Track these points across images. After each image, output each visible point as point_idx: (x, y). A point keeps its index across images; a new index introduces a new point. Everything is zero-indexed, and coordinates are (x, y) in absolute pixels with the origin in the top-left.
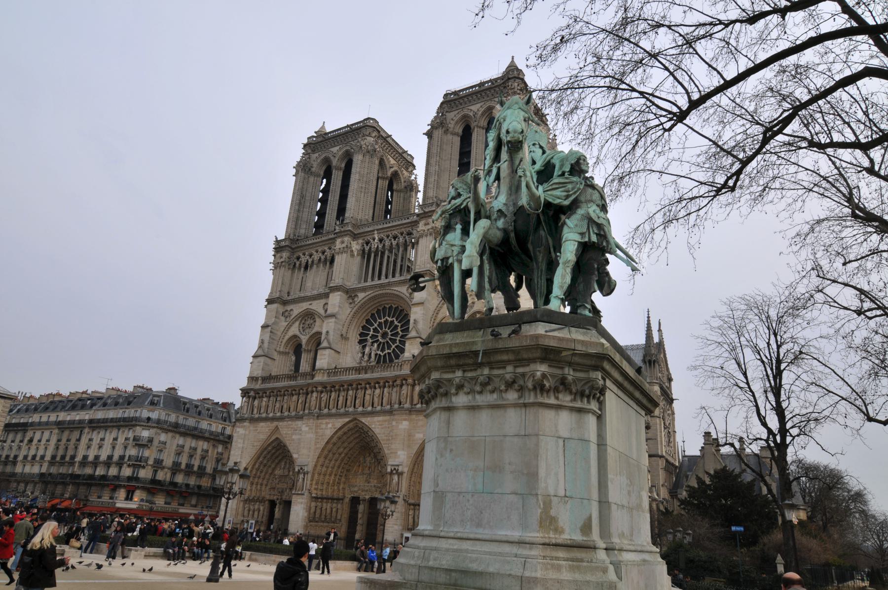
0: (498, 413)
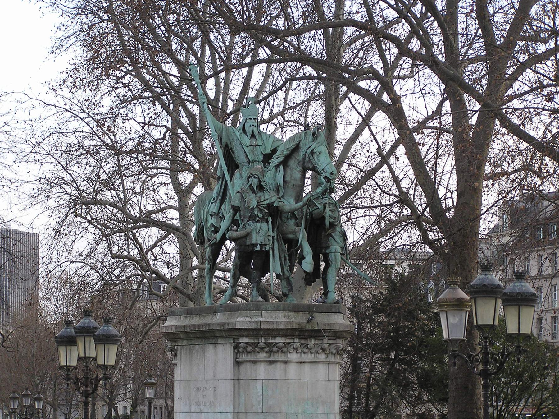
0: (314, 366)
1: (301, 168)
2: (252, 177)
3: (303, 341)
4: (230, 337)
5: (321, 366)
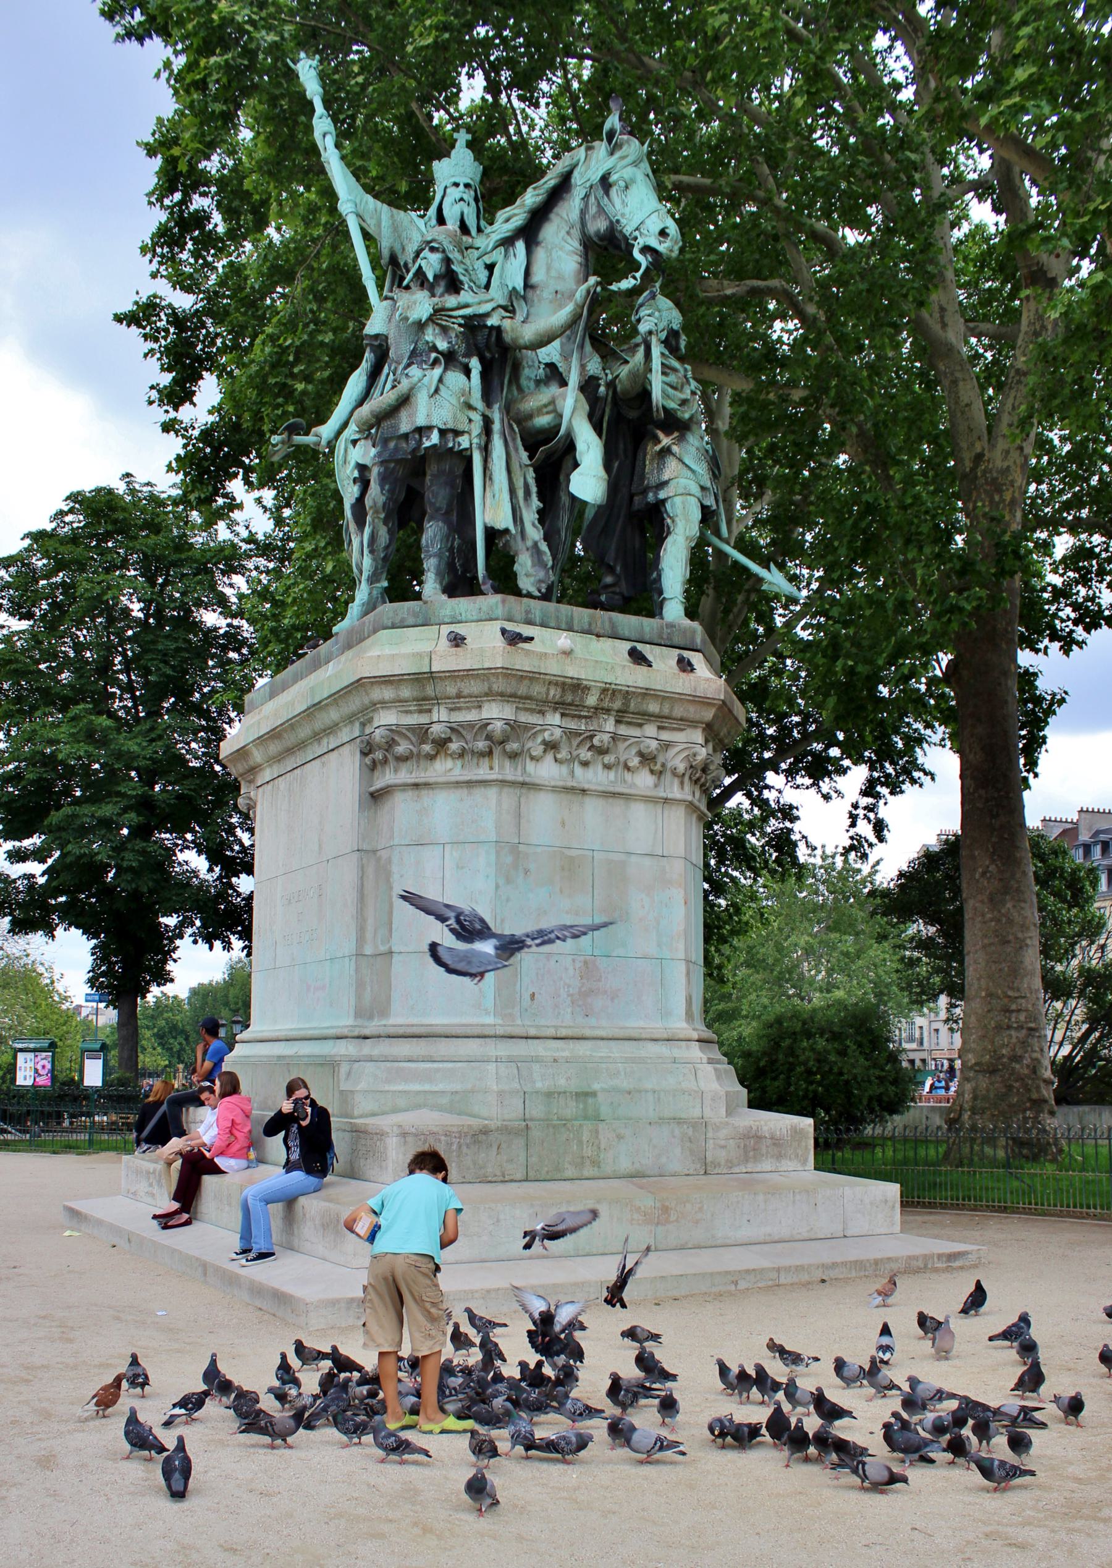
0: (618, 806)
3: (572, 725)
5: (639, 812)
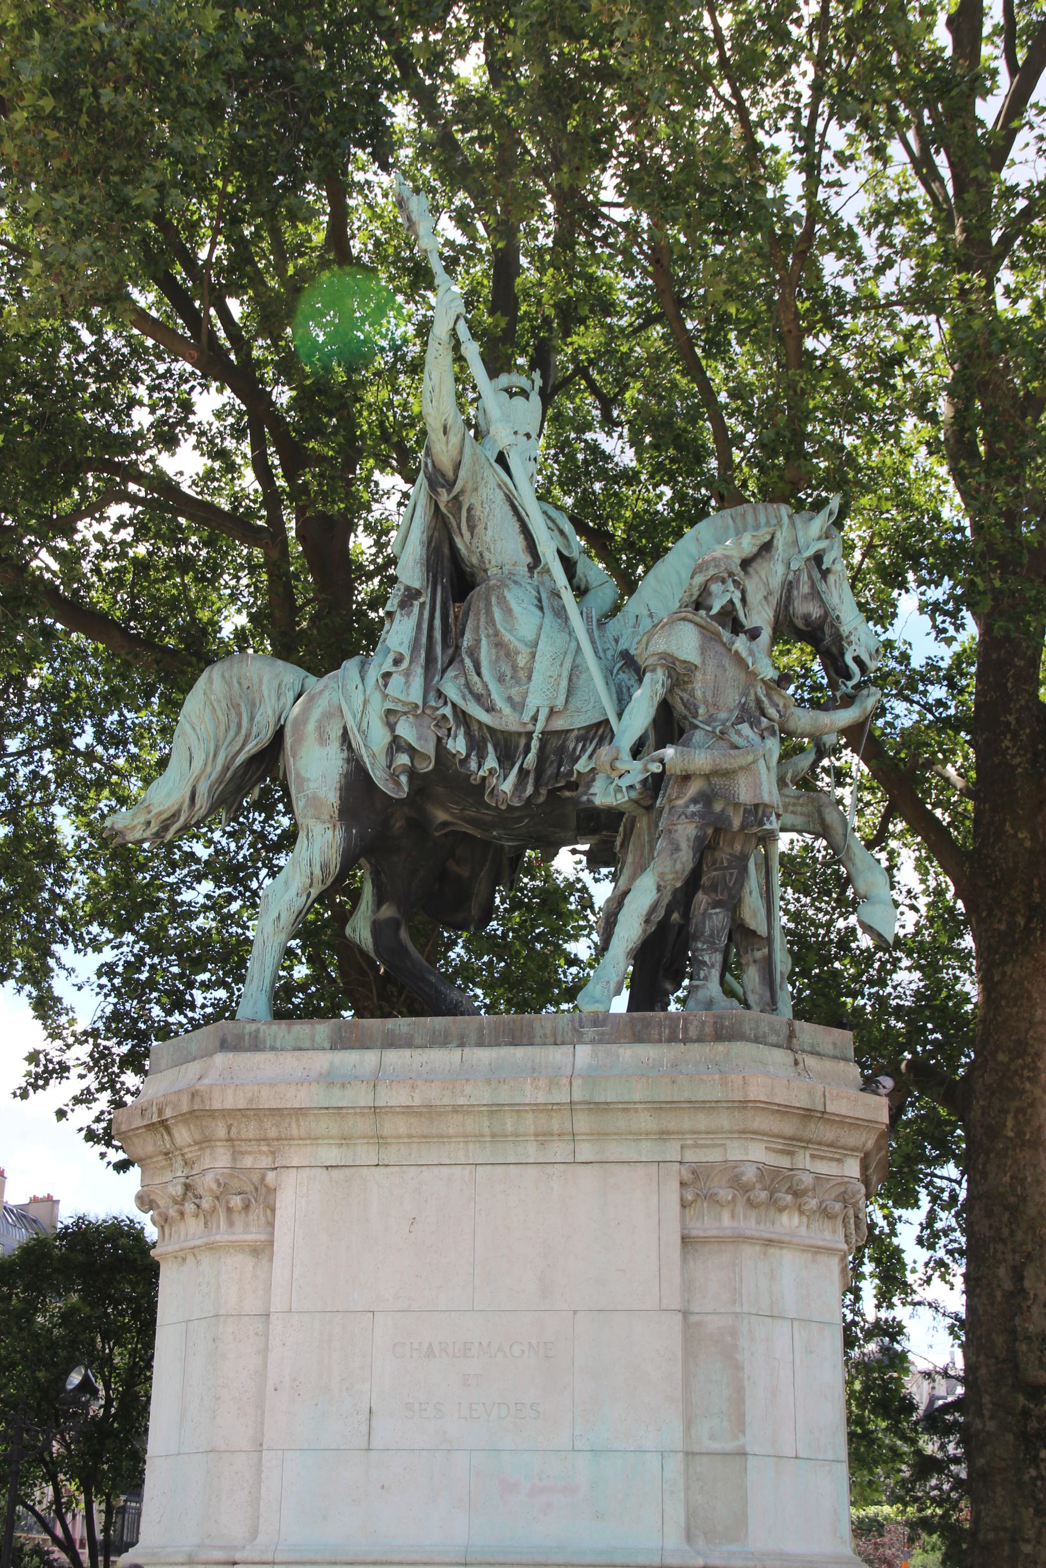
1: (771, 614)
2: (723, 581)
4: (663, 1135)
